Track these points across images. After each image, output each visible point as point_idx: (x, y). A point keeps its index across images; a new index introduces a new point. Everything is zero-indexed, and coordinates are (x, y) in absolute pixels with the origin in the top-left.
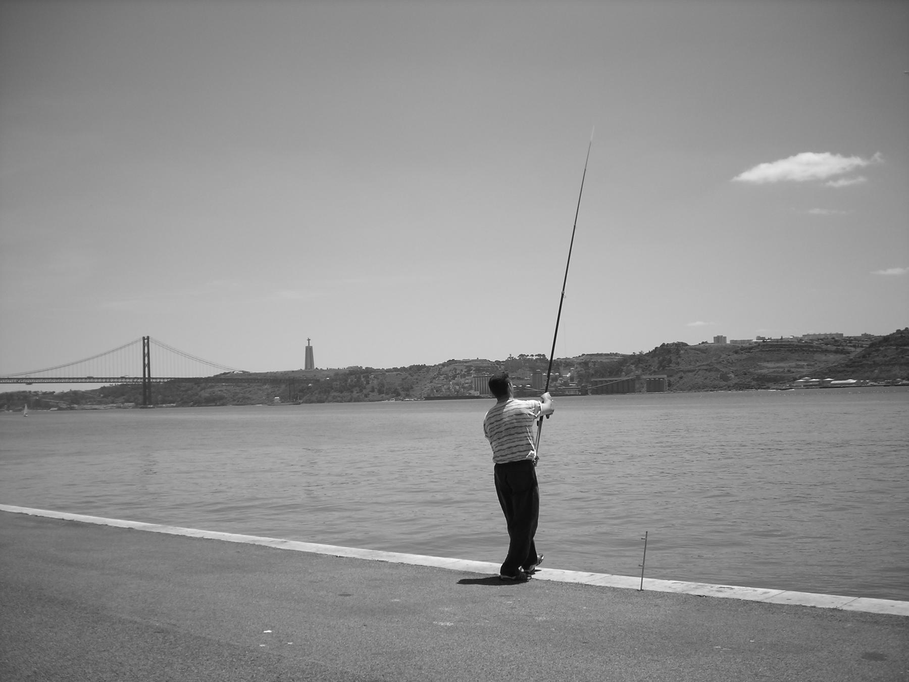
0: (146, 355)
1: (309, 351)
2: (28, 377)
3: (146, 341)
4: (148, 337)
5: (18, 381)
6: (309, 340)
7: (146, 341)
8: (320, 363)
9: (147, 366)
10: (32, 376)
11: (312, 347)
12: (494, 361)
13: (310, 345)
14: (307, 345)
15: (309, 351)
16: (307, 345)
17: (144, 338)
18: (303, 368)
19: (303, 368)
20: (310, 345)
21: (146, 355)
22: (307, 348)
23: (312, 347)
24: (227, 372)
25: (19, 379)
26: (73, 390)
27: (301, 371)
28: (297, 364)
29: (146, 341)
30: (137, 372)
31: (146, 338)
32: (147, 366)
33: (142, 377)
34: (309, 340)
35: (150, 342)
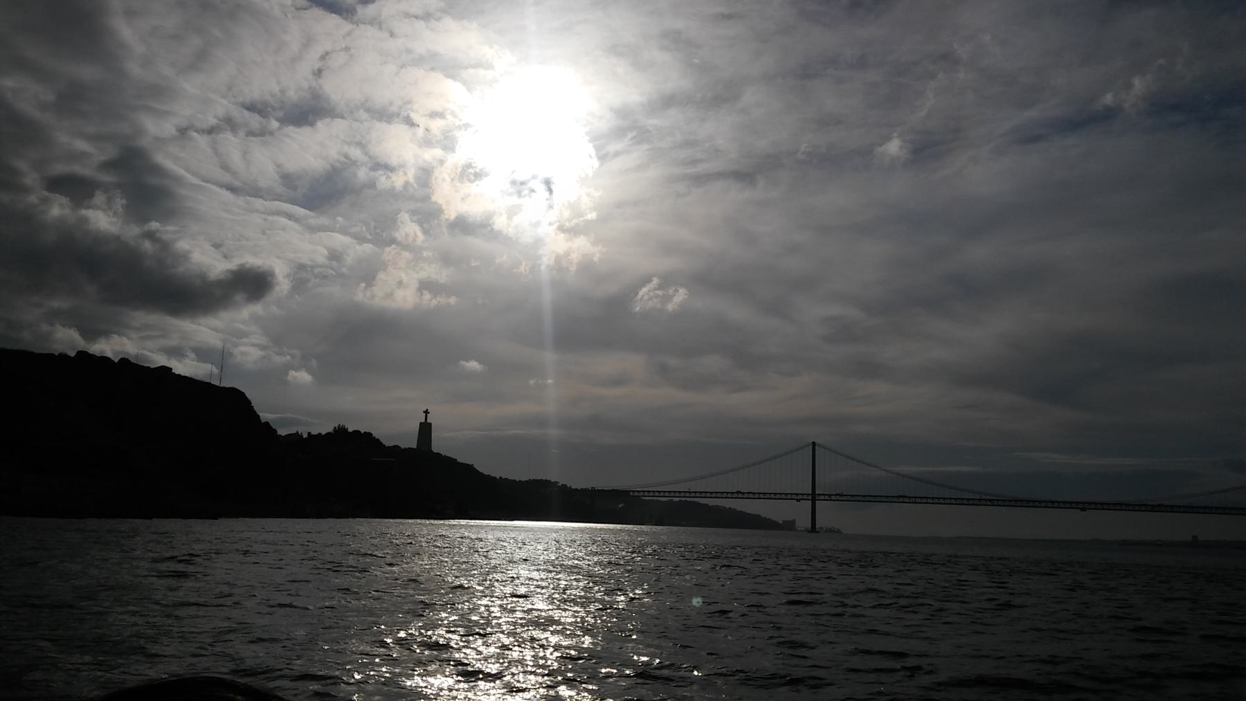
10: (1165, 503)
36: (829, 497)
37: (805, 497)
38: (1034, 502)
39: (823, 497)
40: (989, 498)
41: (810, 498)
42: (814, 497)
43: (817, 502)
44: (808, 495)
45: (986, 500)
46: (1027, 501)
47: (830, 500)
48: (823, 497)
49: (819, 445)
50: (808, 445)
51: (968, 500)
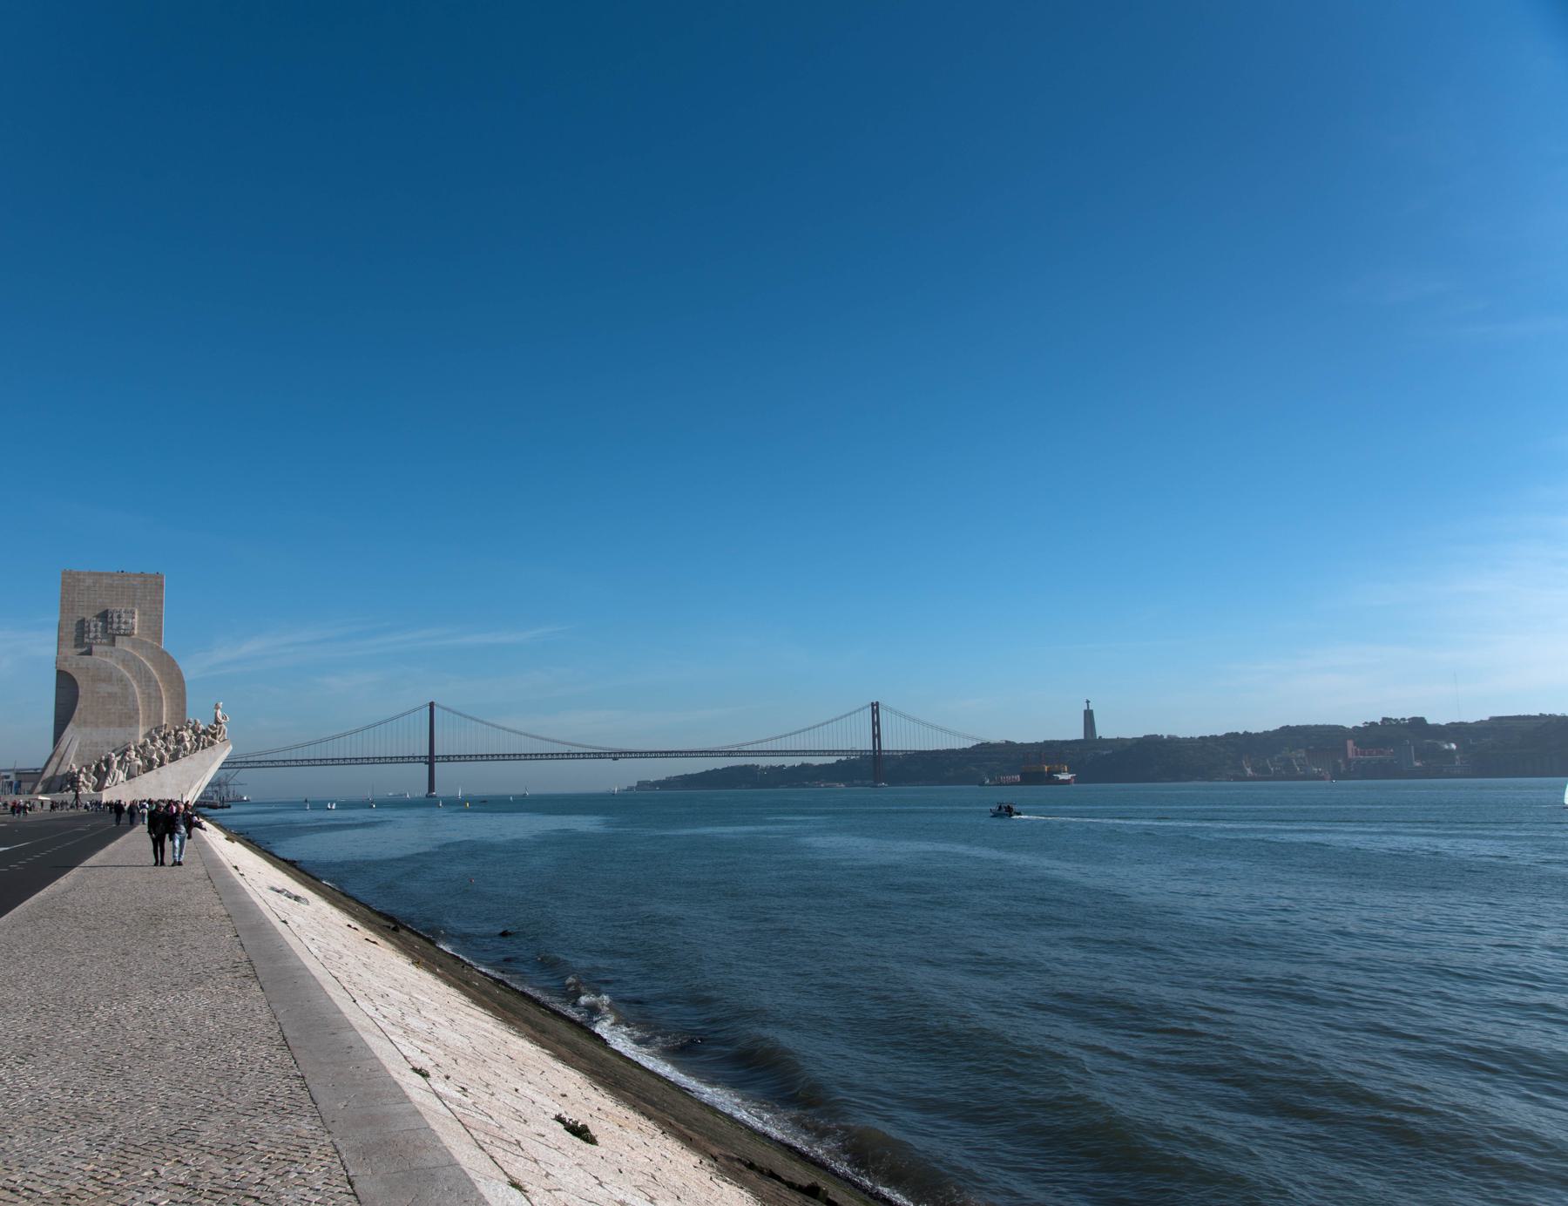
0: (876, 724)
1: (1089, 716)
3: (875, 707)
4: (877, 703)
5: (730, 754)
6: (1088, 702)
7: (875, 707)
8: (1104, 730)
9: (876, 736)
10: (745, 748)
11: (1092, 711)
12: (1351, 727)
13: (1090, 708)
15: (1089, 716)
17: (873, 705)
18: (1082, 737)
19: (1082, 737)
20: (1090, 708)
21: (876, 724)
22: (1085, 711)
23: (1092, 711)
24: (979, 743)
25: (731, 752)
26: (805, 762)
28: (1076, 732)
30: (866, 744)
31: (875, 702)
32: (876, 736)
33: (872, 749)
34: (1088, 702)
35: (880, 710)
36: (448, 759)
37: (422, 759)
38: (636, 753)
39: (440, 759)
40: (595, 751)
42: (431, 760)
43: (436, 764)
44: (426, 757)
45: (595, 753)
46: (630, 753)
47: (449, 761)
48: (440, 759)
49: (438, 706)
50: (426, 706)
51: (579, 754)
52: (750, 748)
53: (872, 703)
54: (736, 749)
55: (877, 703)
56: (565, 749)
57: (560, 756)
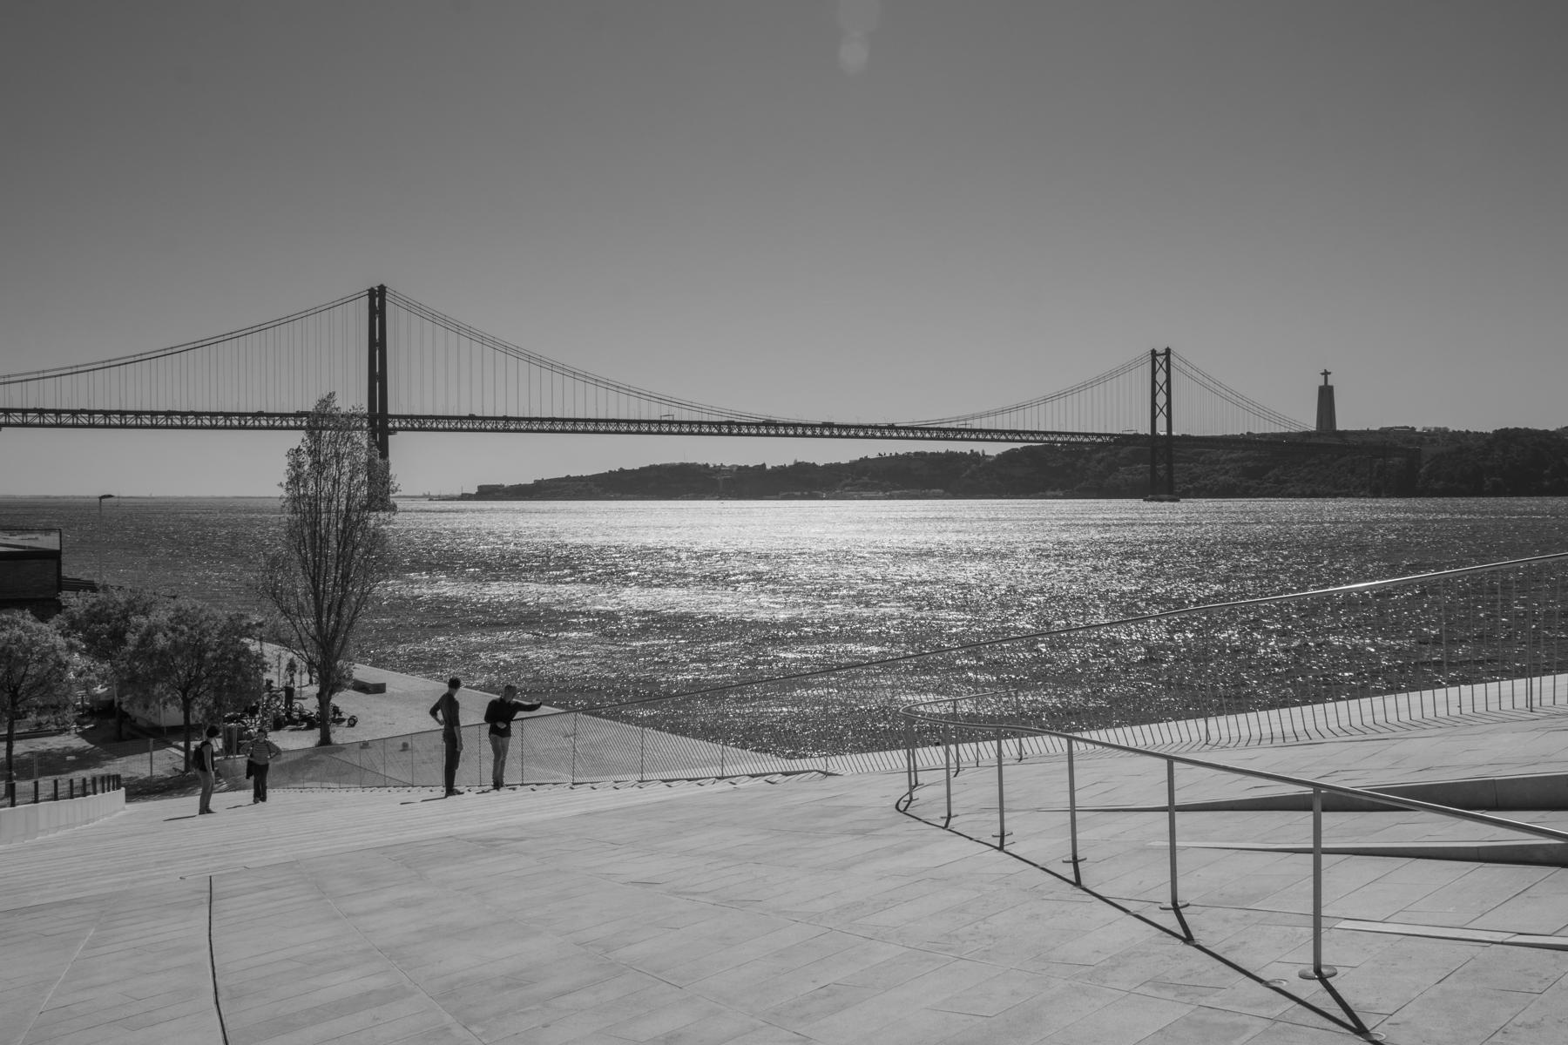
1: (1326, 396)
2: (968, 427)
4: (1168, 352)
6: (1326, 374)
8: (1346, 421)
10: (976, 424)
14: (1323, 384)
15: (1326, 396)
16: (1323, 384)
17: (1154, 353)
20: (1329, 383)
23: (1332, 388)
27: (1307, 434)
28: (1307, 421)
29: (1160, 359)
31: (1160, 349)
34: (1326, 374)
41: (365, 425)
45: (710, 424)
52: (985, 424)
53: (1154, 353)
54: (954, 425)
55: (1168, 352)
56: (655, 412)
57: (30, 418)
